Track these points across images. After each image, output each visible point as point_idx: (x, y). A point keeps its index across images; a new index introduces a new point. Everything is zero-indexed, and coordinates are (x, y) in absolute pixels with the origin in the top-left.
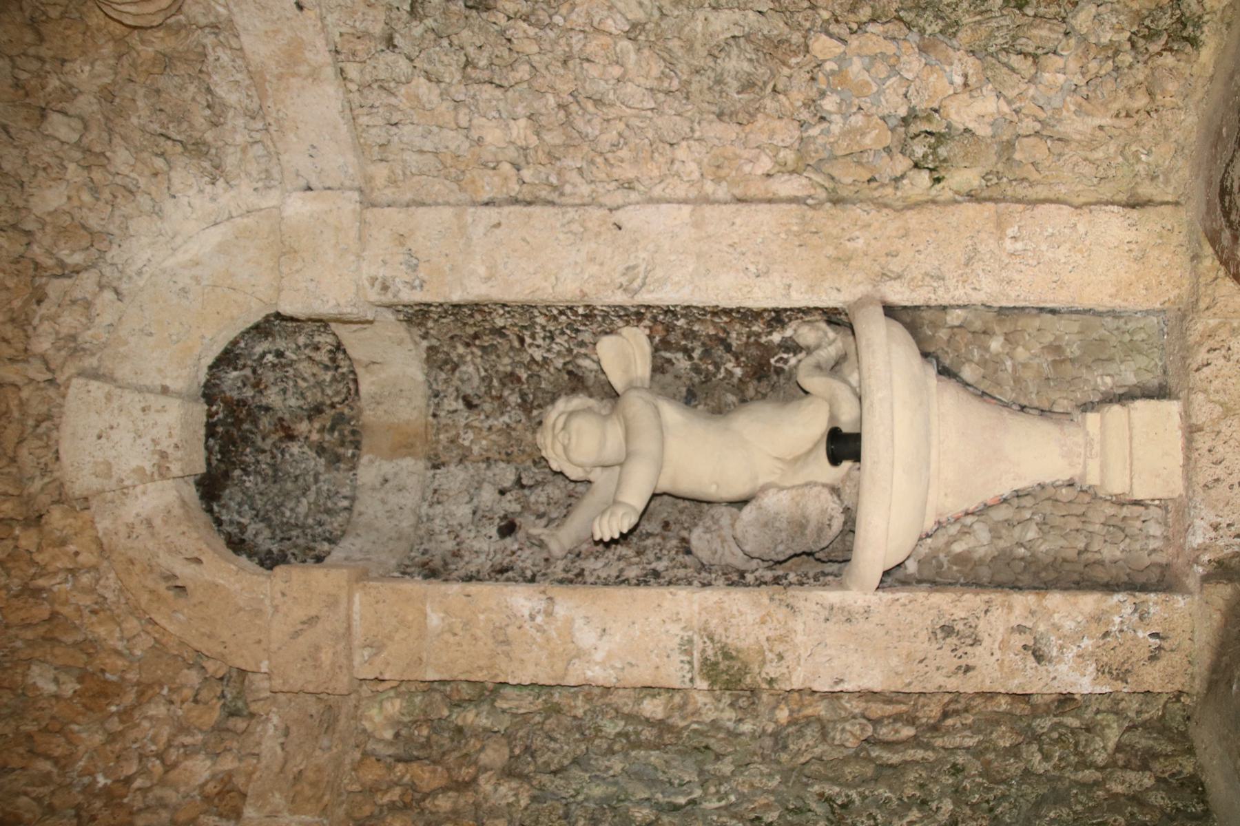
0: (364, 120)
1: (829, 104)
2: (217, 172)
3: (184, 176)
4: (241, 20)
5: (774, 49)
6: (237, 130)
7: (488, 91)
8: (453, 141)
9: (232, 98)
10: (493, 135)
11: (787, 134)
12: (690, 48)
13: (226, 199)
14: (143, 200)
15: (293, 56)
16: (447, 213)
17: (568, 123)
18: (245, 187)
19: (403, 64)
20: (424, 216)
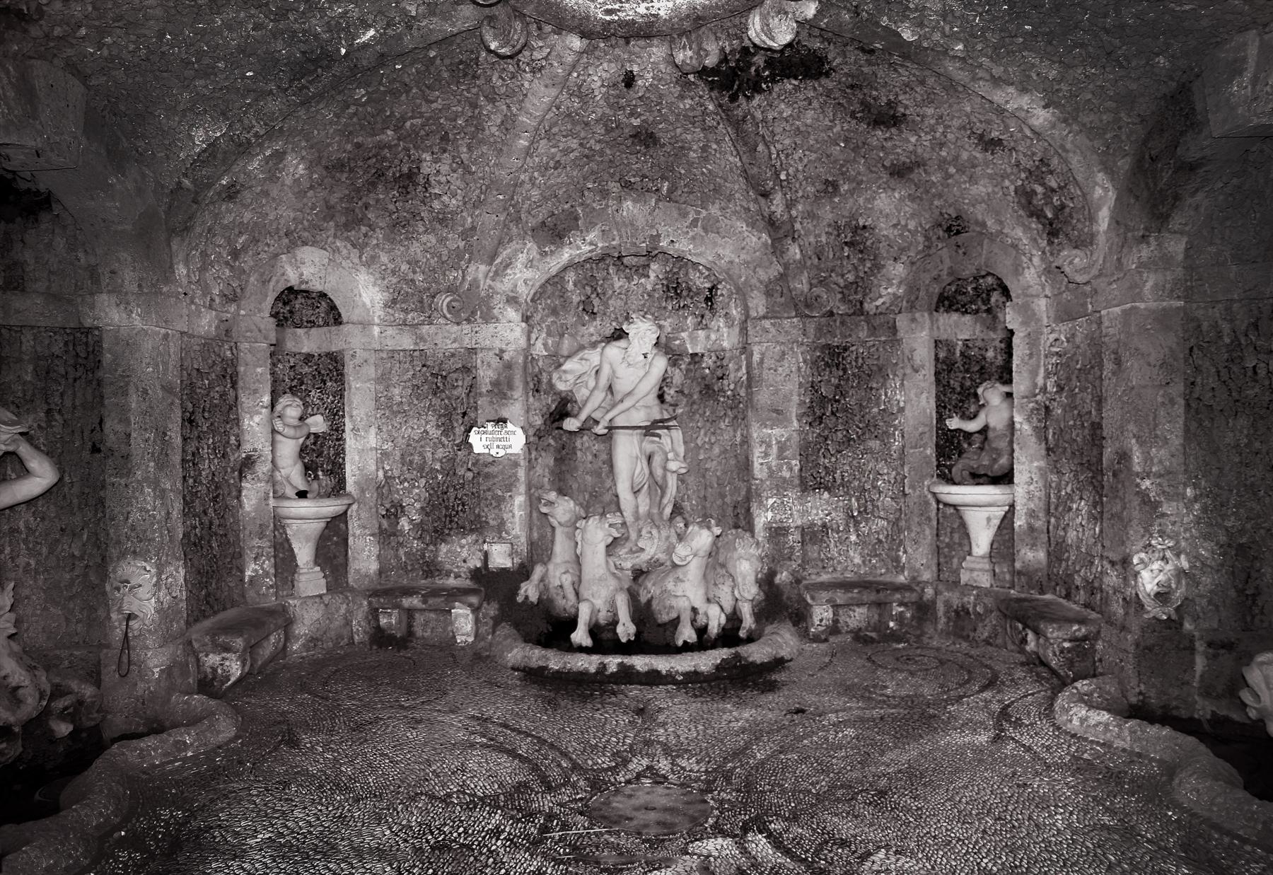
0: (402, 354)
1: (406, 484)
2: (386, 306)
3: (386, 296)
4: (433, 327)
5: (421, 469)
6: (399, 316)
7: (410, 391)
8: (395, 380)
9: (409, 316)
10: (397, 391)
11: (396, 473)
12: (422, 447)
13: (379, 306)
14: (379, 282)
15: (422, 339)
16: (373, 376)
17: (399, 412)
18: (381, 313)
19: (418, 369)
20: (372, 369)
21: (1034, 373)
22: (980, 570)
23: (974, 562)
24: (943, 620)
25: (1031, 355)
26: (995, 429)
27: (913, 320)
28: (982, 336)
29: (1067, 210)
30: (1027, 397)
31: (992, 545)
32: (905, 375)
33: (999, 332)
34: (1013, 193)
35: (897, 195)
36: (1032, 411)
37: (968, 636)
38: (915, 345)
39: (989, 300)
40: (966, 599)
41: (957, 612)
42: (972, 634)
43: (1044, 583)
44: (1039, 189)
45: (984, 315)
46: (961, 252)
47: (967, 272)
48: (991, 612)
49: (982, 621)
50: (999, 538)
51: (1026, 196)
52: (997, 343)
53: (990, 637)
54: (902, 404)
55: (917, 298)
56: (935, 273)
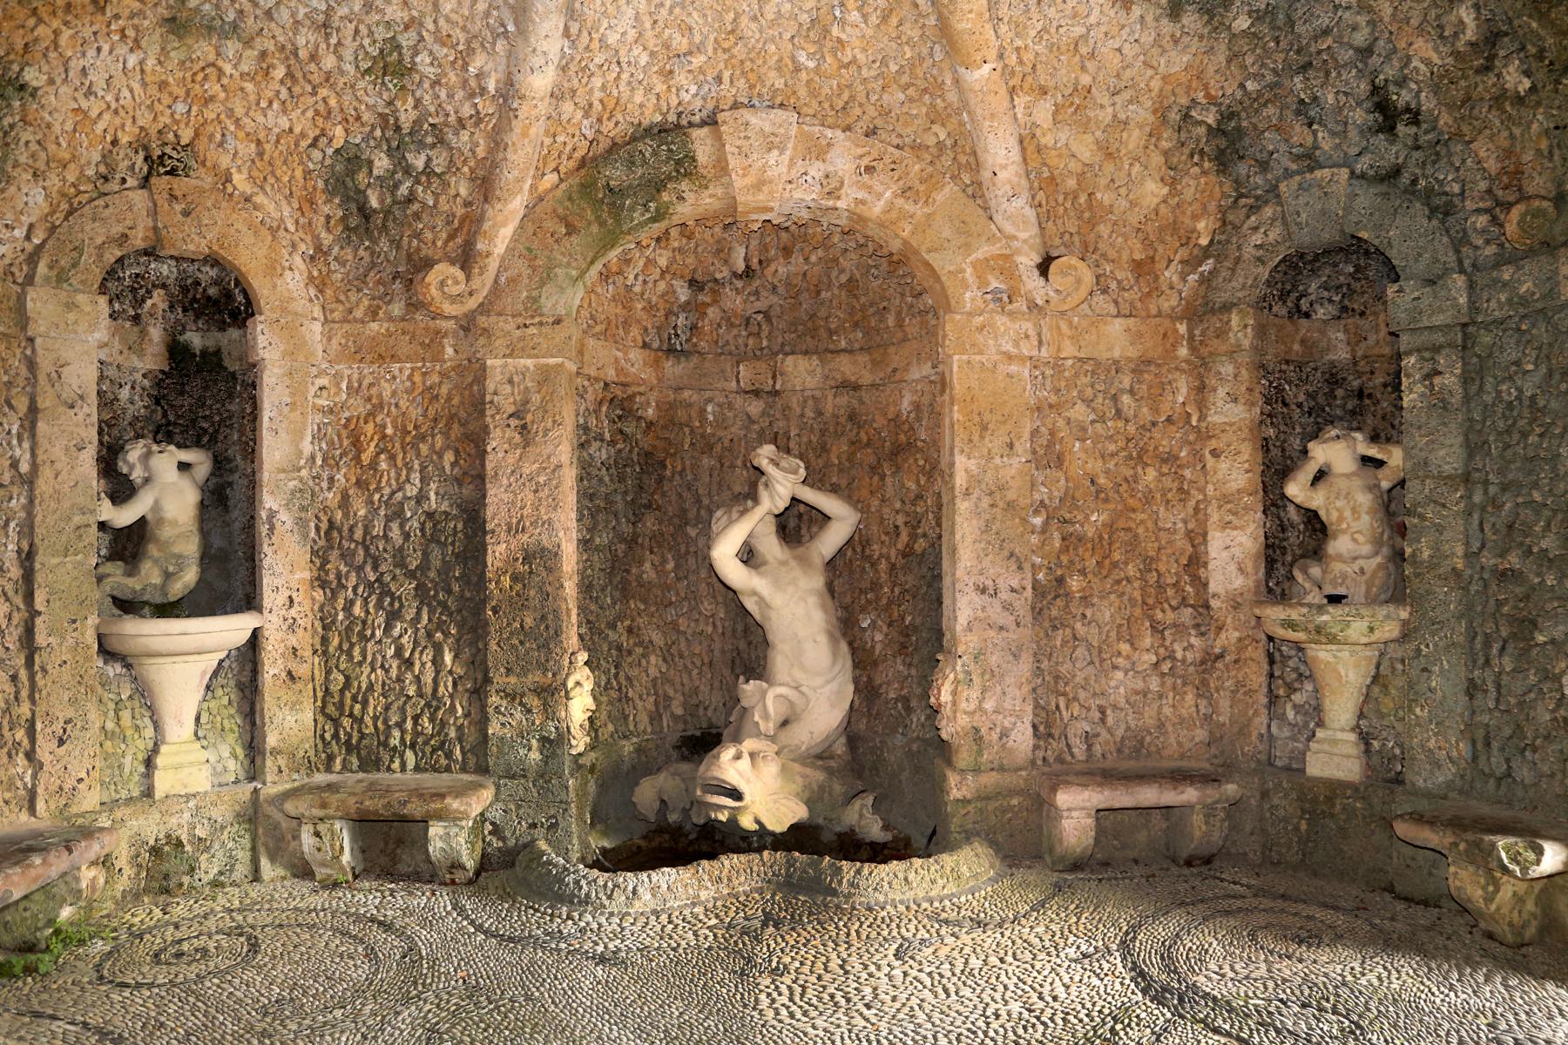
21: (298, 435)
22: (191, 764)
23: (177, 753)
24: (128, 871)
25: (292, 406)
26: (174, 523)
27: (71, 306)
28: (120, 359)
29: (416, 207)
30: (284, 471)
31: (198, 719)
32: (33, 410)
33: (148, 359)
34: (330, 151)
35: (132, 61)
36: (293, 493)
37: (181, 885)
38: (67, 354)
39: (143, 301)
40: (174, 820)
41: (155, 851)
42: (186, 880)
43: (313, 759)
44: (382, 163)
45: (128, 324)
46: (178, 207)
47: (192, 247)
48: (223, 828)
49: (207, 849)
50: (213, 704)
51: (352, 160)
52: (139, 377)
53: (221, 873)
54: (24, 467)
55: (74, 265)
56: (117, 229)
